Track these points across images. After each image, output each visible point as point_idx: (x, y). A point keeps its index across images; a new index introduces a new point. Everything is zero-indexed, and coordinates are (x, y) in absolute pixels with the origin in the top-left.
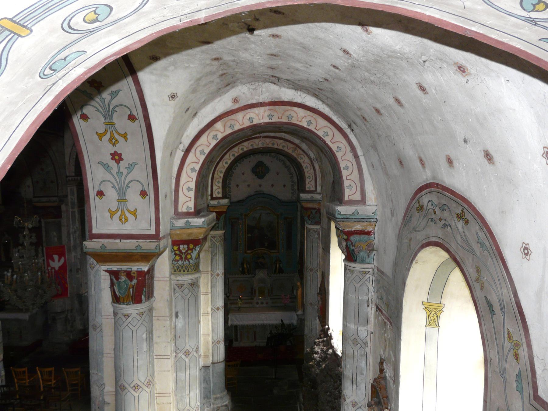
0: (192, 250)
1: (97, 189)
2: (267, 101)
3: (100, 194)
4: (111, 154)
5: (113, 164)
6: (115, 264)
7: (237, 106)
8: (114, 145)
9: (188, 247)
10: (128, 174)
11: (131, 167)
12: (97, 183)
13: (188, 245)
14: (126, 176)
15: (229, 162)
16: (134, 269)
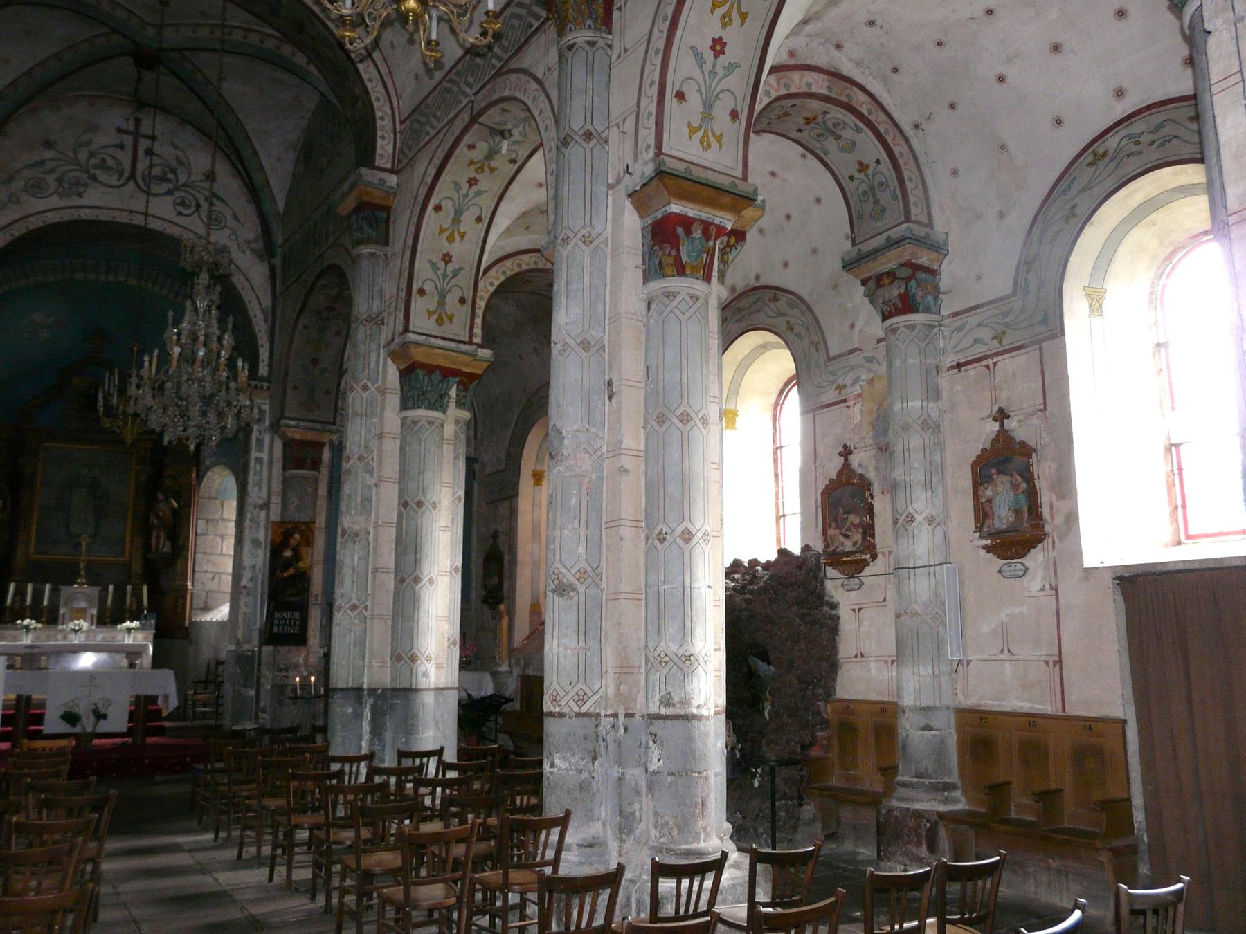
0: (731, 247)
1: (677, 88)
2: (826, 67)
3: (680, 96)
4: (714, 40)
5: (709, 55)
6: (692, 205)
7: (792, 62)
8: (724, 26)
9: (728, 242)
10: (724, 77)
11: (731, 68)
12: (679, 79)
13: (729, 238)
14: (720, 81)
15: (497, 283)
16: (717, 221)
